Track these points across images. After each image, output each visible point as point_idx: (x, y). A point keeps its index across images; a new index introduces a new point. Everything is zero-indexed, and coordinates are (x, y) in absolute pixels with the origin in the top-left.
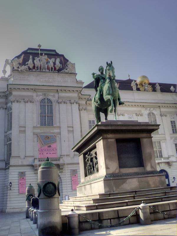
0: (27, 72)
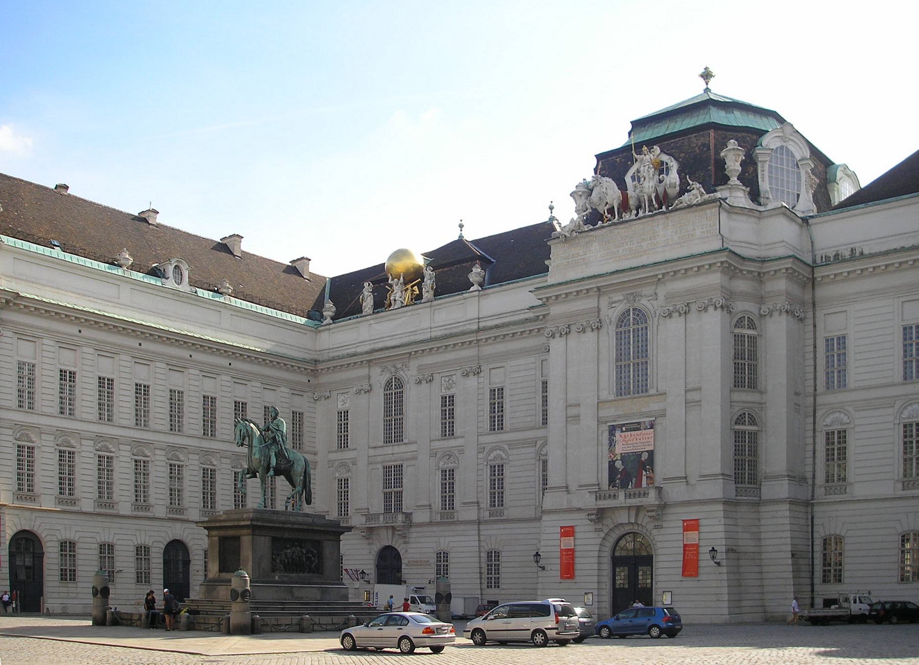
0: (584, 234)
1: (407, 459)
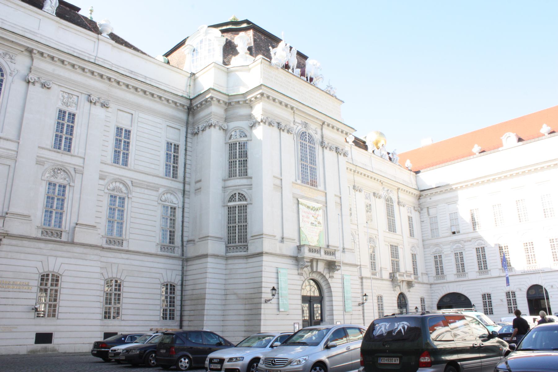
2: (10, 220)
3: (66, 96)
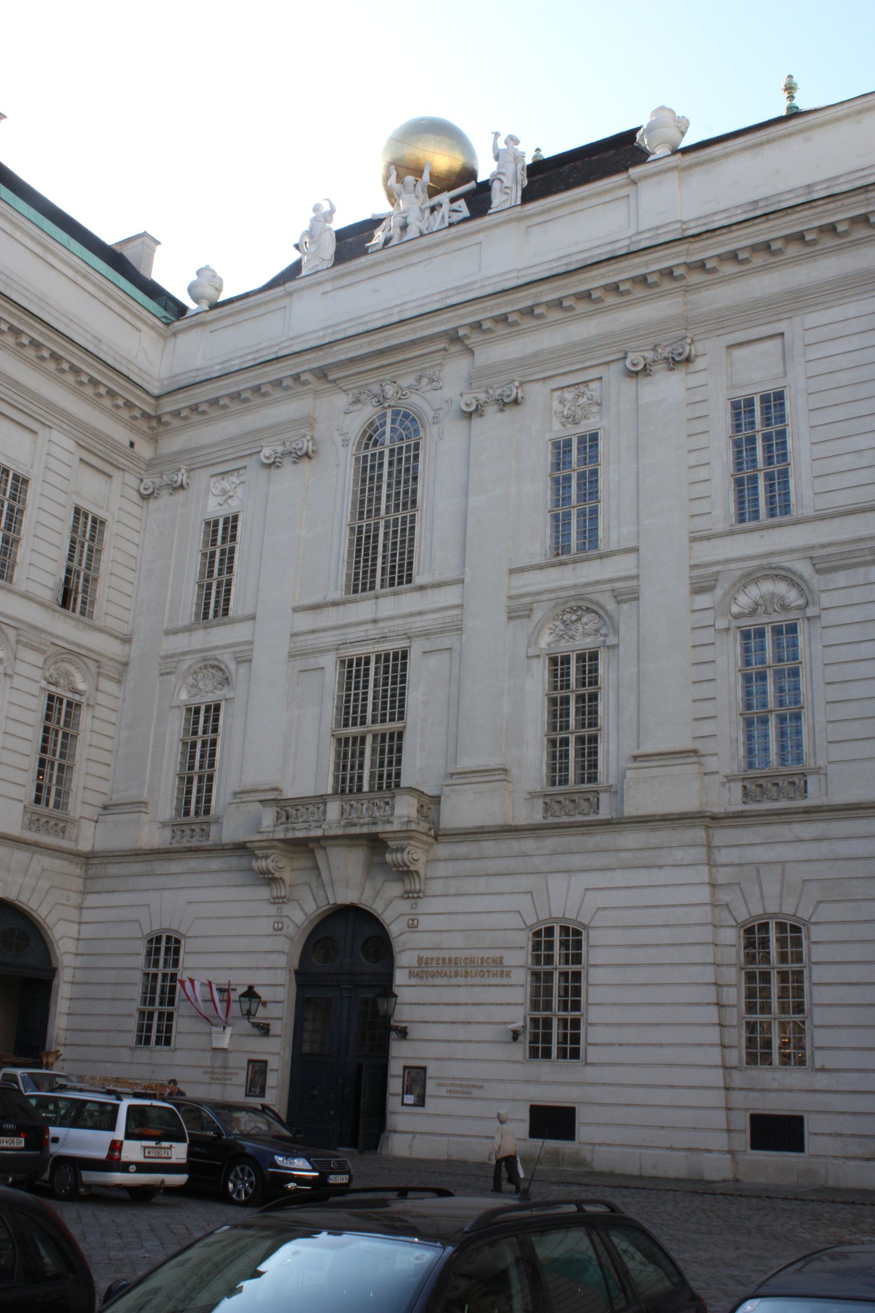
1: (426, 634)
2: (453, 791)
3: (569, 395)
